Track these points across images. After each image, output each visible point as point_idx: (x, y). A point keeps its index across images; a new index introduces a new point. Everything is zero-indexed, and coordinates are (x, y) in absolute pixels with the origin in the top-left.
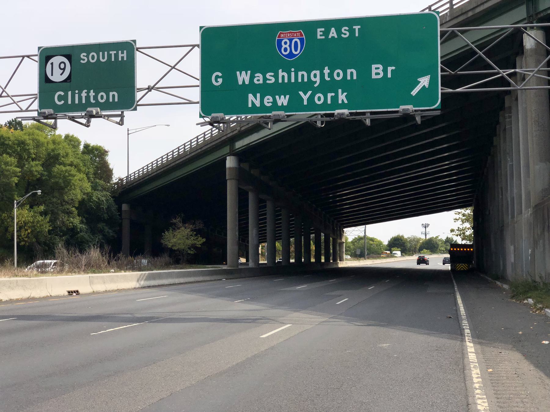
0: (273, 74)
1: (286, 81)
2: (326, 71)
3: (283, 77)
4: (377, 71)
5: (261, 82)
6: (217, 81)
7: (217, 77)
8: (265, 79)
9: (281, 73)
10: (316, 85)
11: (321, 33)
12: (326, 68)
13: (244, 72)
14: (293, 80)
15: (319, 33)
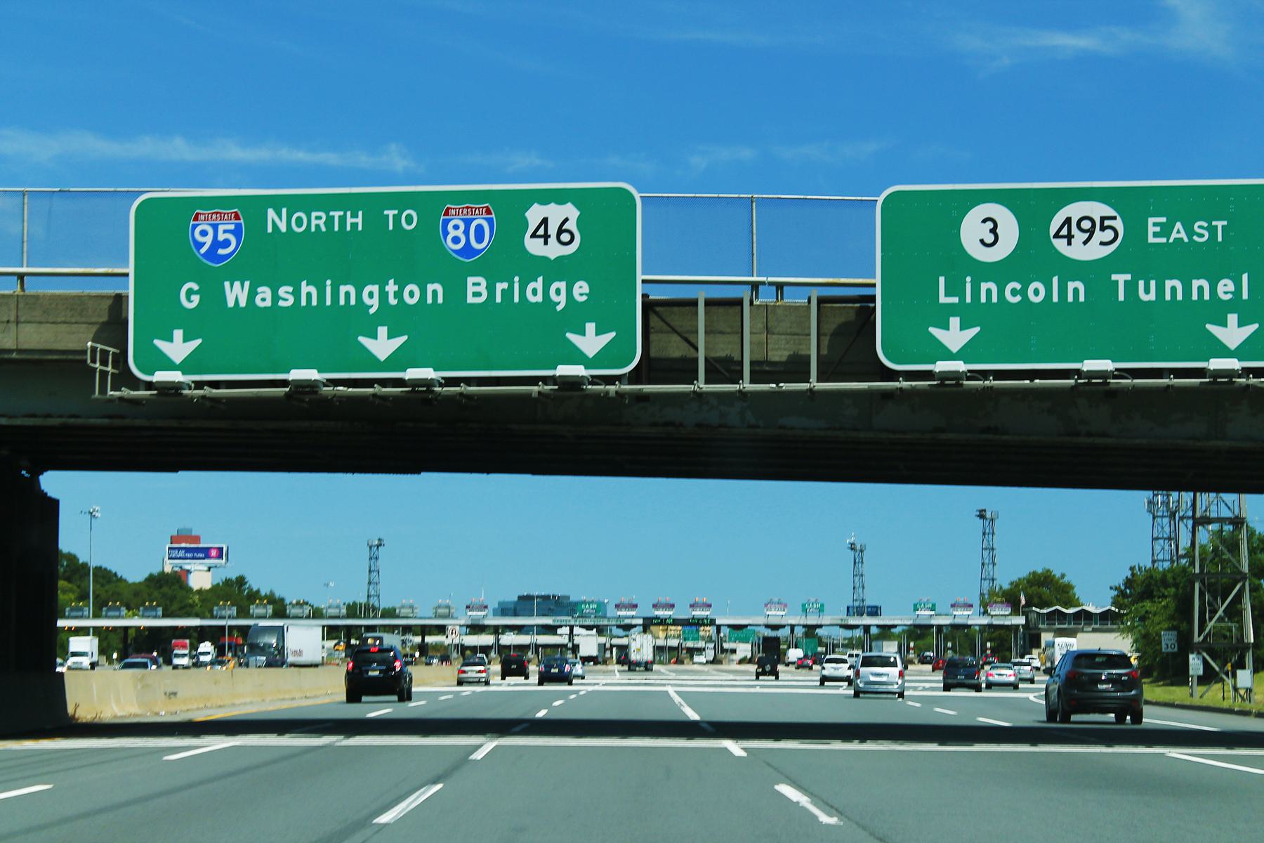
0: (290, 289)
1: (314, 303)
2: (391, 287)
3: (309, 295)
4: (477, 289)
5: (268, 303)
6: (189, 300)
7: (190, 292)
8: (276, 298)
9: (305, 288)
11: (1158, 229)
12: (391, 282)
13: (237, 284)
14: (328, 303)
15: (1152, 229)
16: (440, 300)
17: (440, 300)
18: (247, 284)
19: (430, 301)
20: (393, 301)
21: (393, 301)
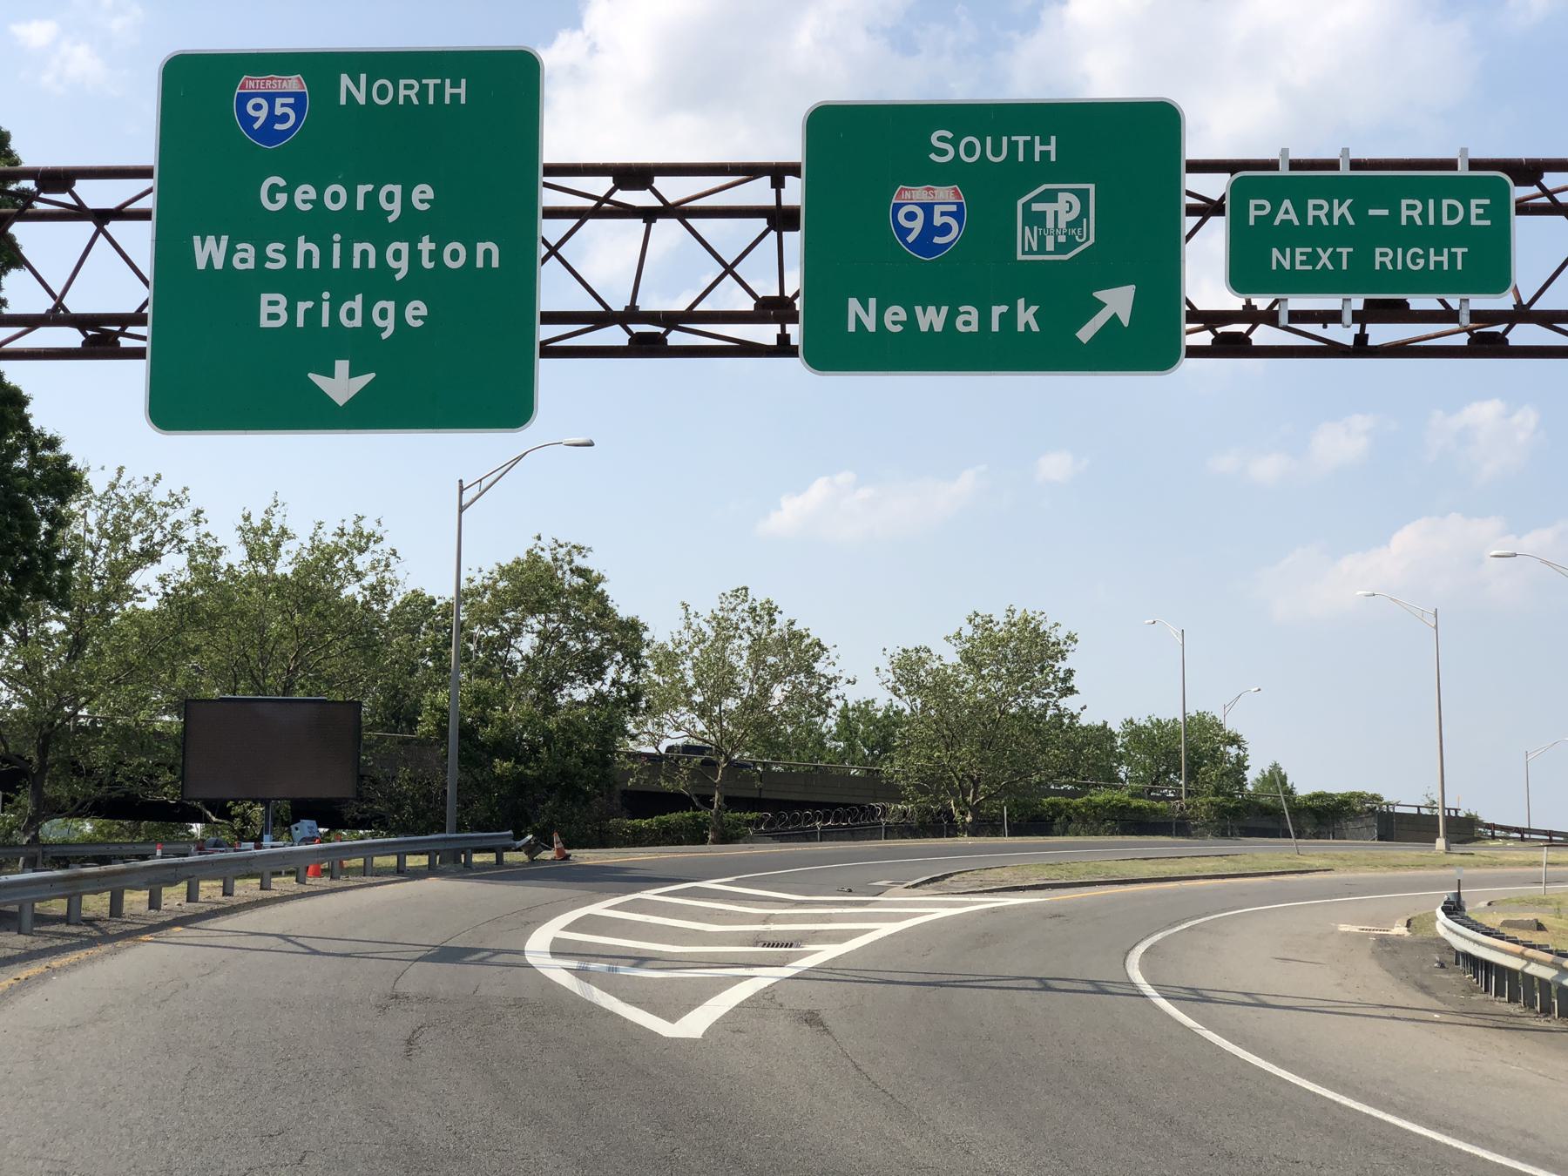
0: (281, 247)
1: (316, 264)
2: (426, 245)
3: (308, 254)
5: (251, 265)
8: (261, 258)
9: (302, 245)
10: (399, 277)
12: (426, 239)
13: (211, 239)
14: (336, 264)
16: (495, 263)
17: (495, 263)
18: (225, 239)
19: (480, 264)
20: (427, 264)
21: (427, 264)
